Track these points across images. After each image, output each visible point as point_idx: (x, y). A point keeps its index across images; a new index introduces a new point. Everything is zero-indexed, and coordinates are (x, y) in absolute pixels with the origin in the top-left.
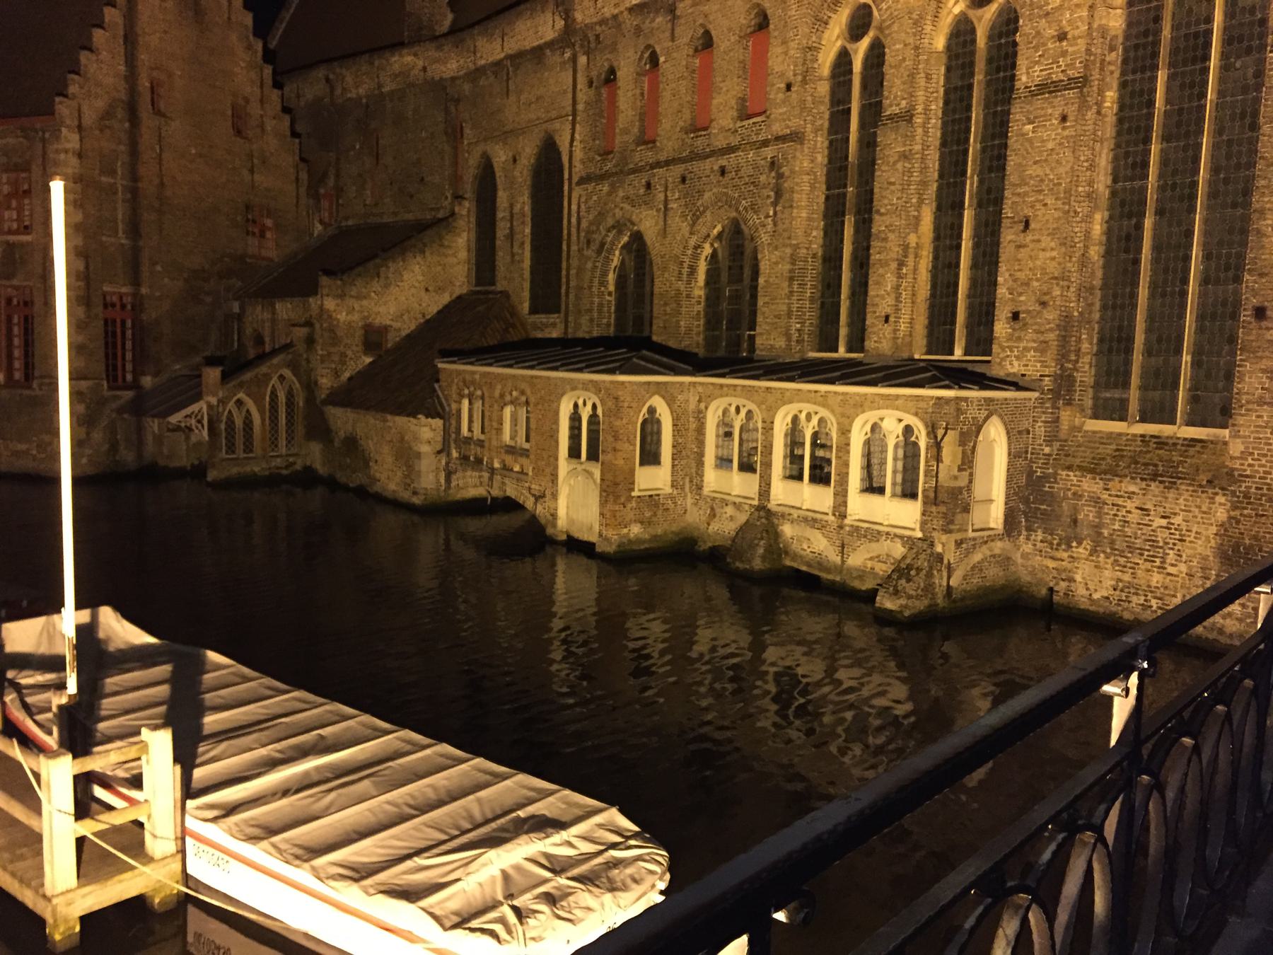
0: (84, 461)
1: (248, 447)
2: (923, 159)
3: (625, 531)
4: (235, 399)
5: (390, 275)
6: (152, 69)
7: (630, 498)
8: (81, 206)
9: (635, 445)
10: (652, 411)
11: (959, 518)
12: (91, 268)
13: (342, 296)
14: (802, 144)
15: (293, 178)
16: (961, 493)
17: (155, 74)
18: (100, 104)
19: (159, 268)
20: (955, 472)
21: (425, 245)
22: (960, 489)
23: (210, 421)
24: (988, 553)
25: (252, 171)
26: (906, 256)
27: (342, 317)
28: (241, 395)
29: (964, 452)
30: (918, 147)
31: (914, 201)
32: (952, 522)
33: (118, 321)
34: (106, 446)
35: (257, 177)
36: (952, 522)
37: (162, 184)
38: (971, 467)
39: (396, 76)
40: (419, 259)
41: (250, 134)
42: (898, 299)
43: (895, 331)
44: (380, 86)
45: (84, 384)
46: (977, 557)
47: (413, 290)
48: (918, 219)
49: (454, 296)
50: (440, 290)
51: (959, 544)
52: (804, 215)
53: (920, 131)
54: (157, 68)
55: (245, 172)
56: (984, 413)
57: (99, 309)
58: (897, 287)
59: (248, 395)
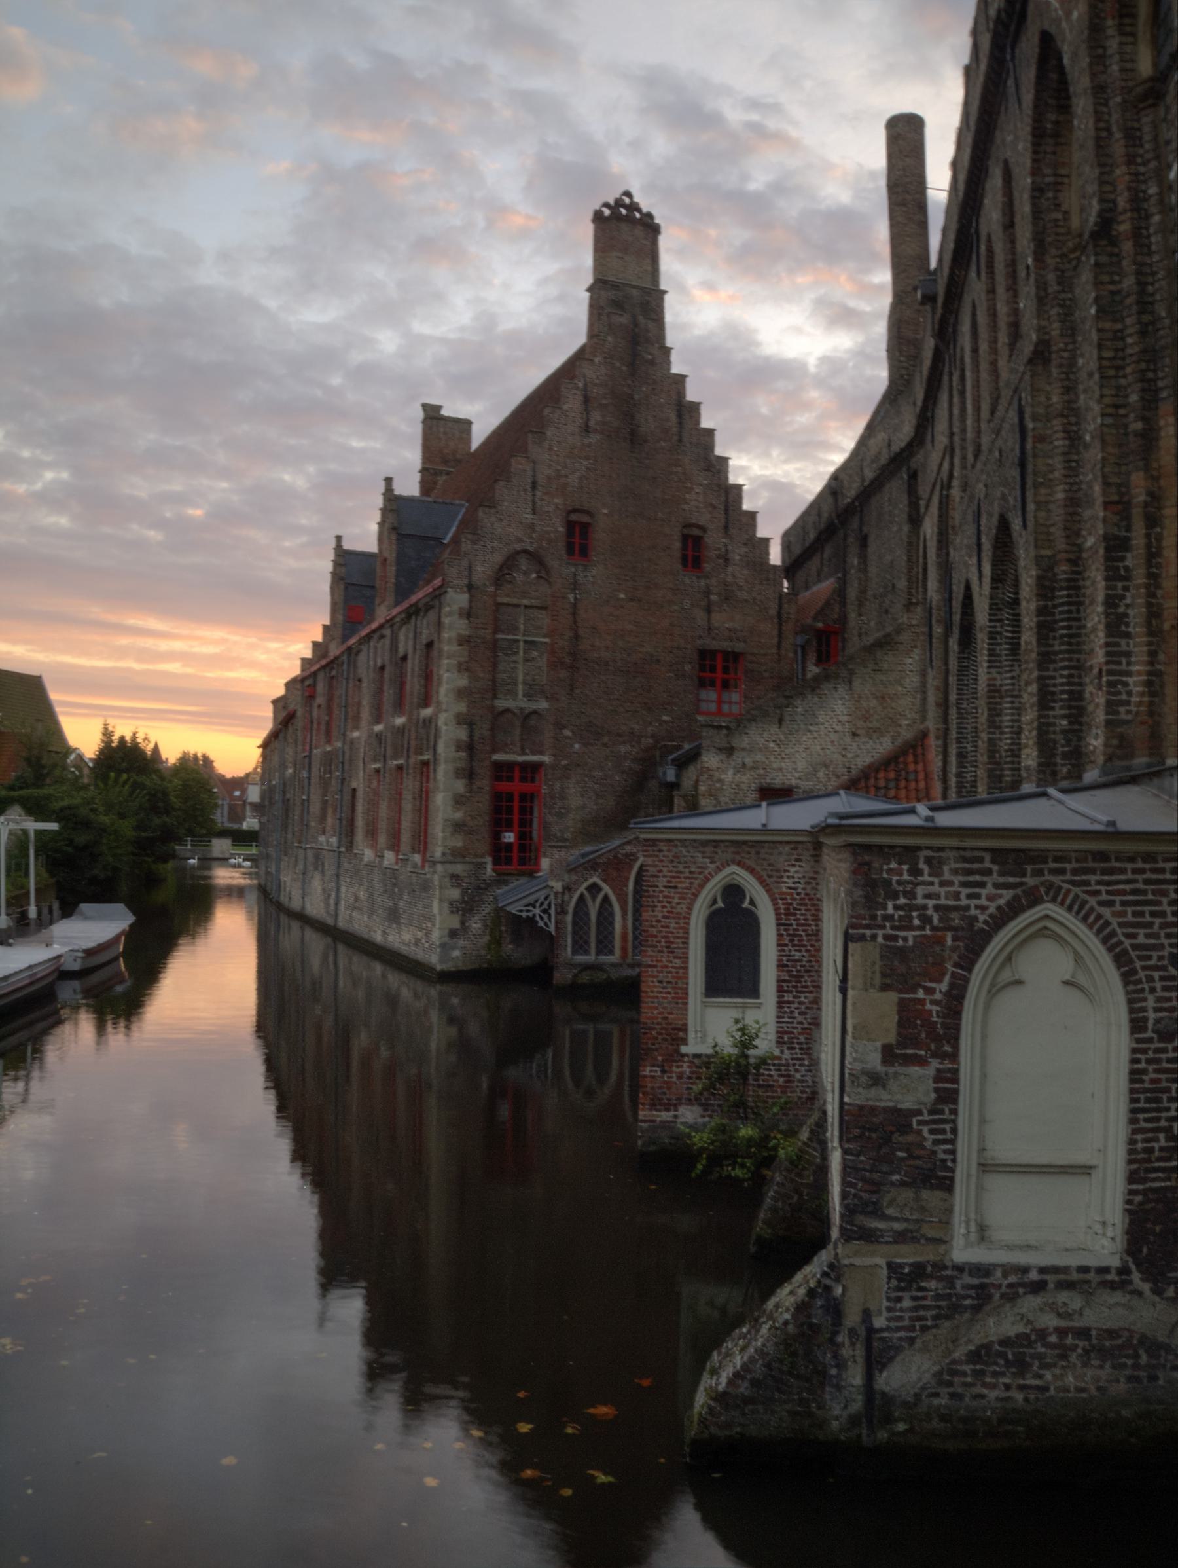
0: (456, 953)
1: (605, 945)
2: (1145, 304)
3: (665, 1116)
4: (586, 885)
5: (798, 718)
6: (569, 512)
7: (675, 1056)
8: (467, 670)
9: (685, 958)
10: (733, 892)
11: (899, 1204)
12: (476, 738)
13: (730, 751)
14: (1046, 362)
15: (773, 612)
16: (905, 1128)
17: (574, 517)
18: (497, 558)
19: (567, 733)
20: (874, 1060)
21: (852, 673)
22: (900, 1119)
23: (557, 913)
24: (1050, 1321)
25: (708, 610)
26: (1128, 529)
27: (728, 776)
28: (595, 879)
29: (908, 1014)
30: (1129, 282)
31: (1134, 398)
32: (876, 1212)
33: (516, 798)
34: (487, 938)
35: (718, 618)
36: (876, 1212)
37: (577, 637)
38: (954, 1056)
39: (873, 462)
40: (842, 690)
41: (707, 567)
42: (1116, 625)
43: (1111, 707)
44: (863, 480)
45: (459, 869)
46: (1000, 1325)
47: (833, 736)
48: (1149, 437)
49: (899, 741)
50: (875, 732)
51: (908, 1278)
52: (1060, 495)
53: (1127, 247)
54: (575, 511)
55: (700, 615)
56: (992, 897)
57: (485, 783)
58: (1111, 602)
59: (604, 880)
